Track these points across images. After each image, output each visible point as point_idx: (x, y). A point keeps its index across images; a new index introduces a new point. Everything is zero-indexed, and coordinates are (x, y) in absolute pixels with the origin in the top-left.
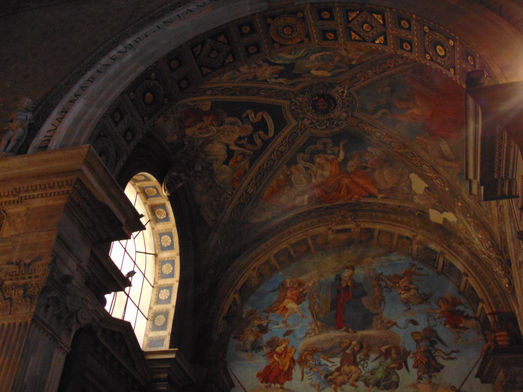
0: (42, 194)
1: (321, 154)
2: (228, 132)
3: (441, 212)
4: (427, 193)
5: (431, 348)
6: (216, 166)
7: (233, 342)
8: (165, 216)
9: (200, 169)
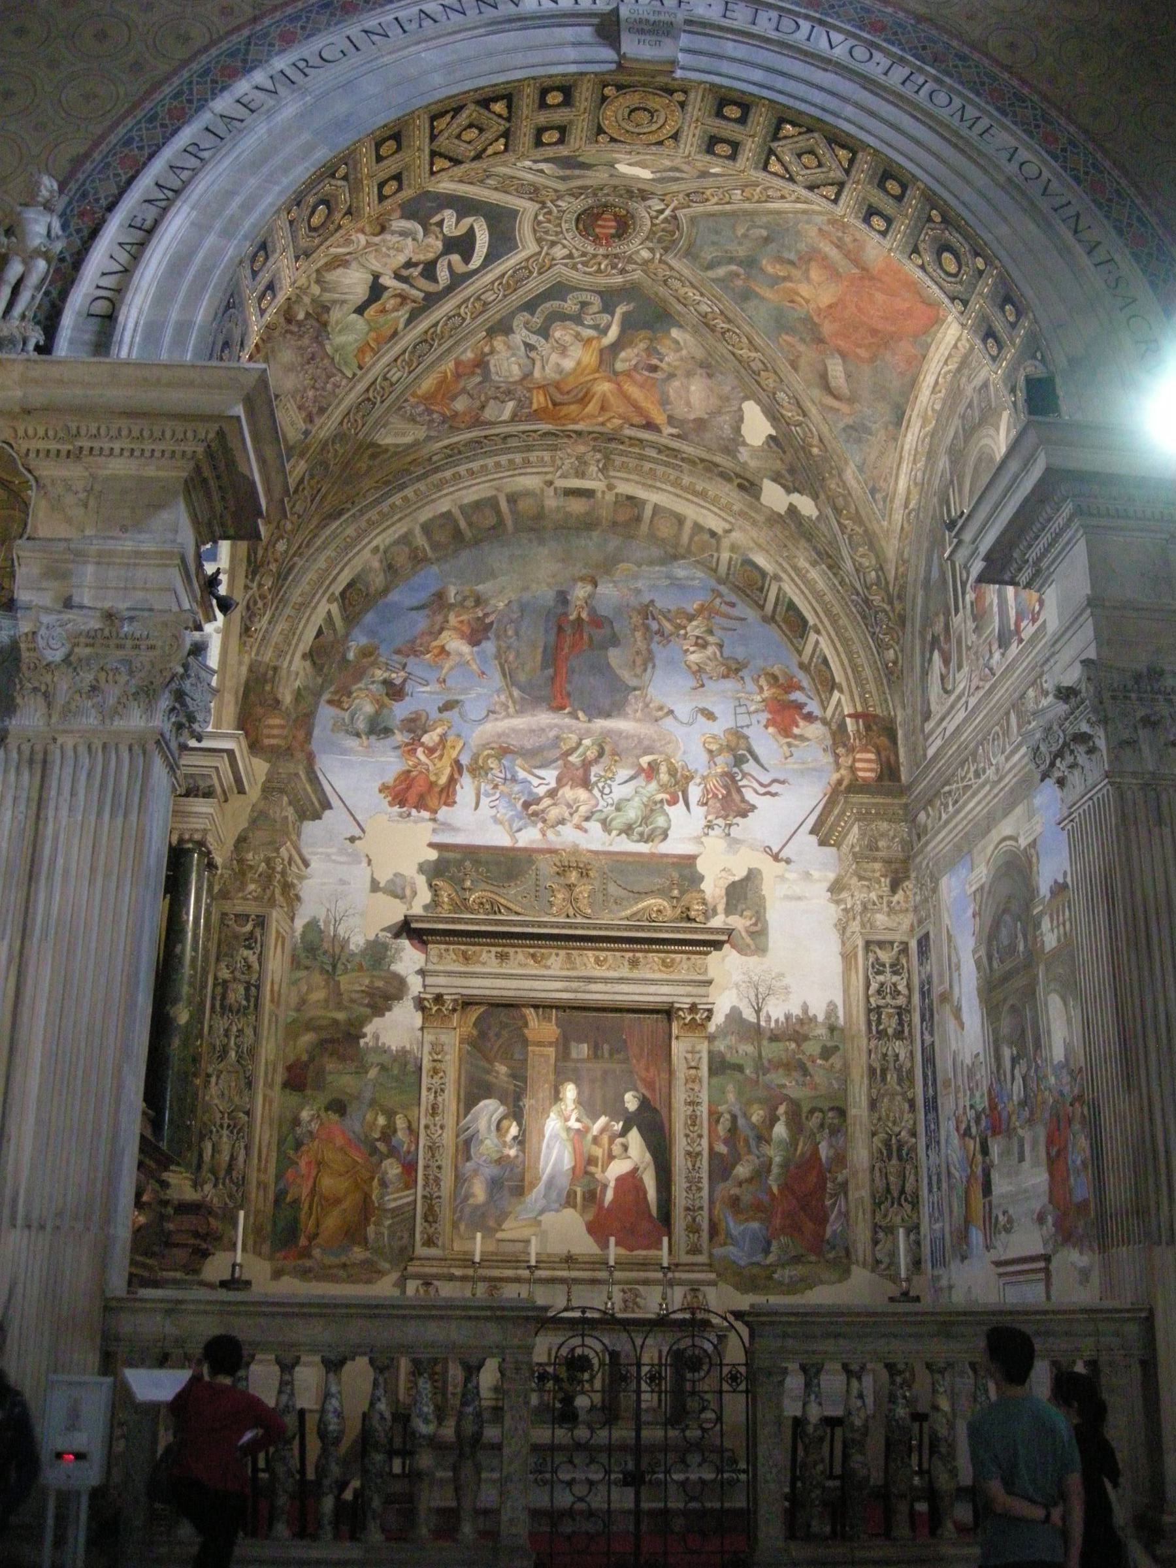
0: (132, 450)
3: (789, 491)
5: (735, 770)
6: (335, 315)
7: (326, 714)
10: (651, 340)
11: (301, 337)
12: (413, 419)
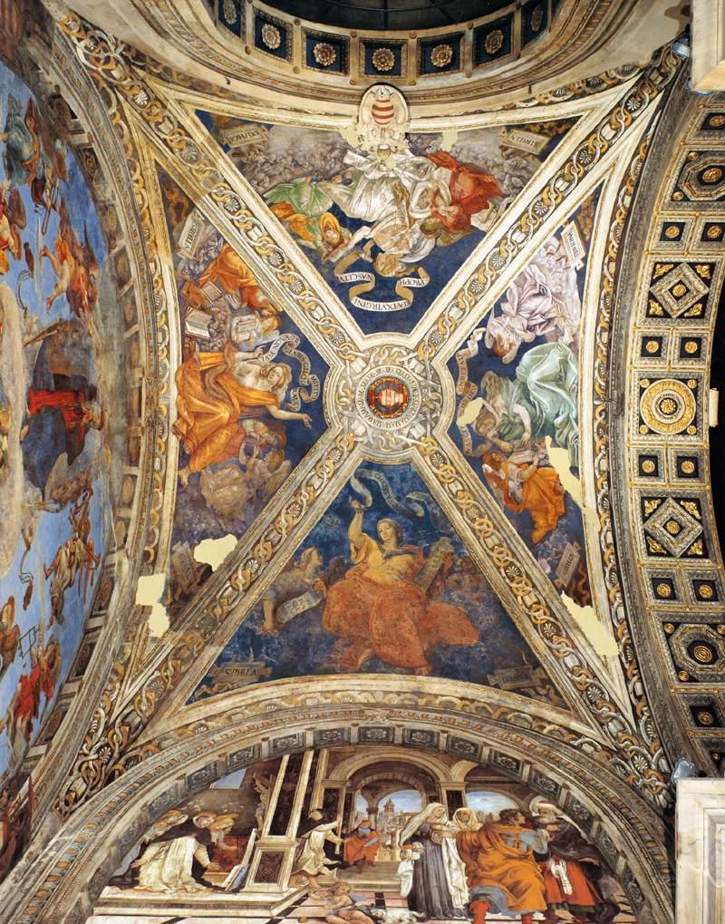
1: (291, 377)
2: (402, 235)
4: (198, 570)
6: (337, 190)
8: (317, 60)
9: (347, 161)
10: (278, 447)
11: (325, 158)
12: (205, 246)
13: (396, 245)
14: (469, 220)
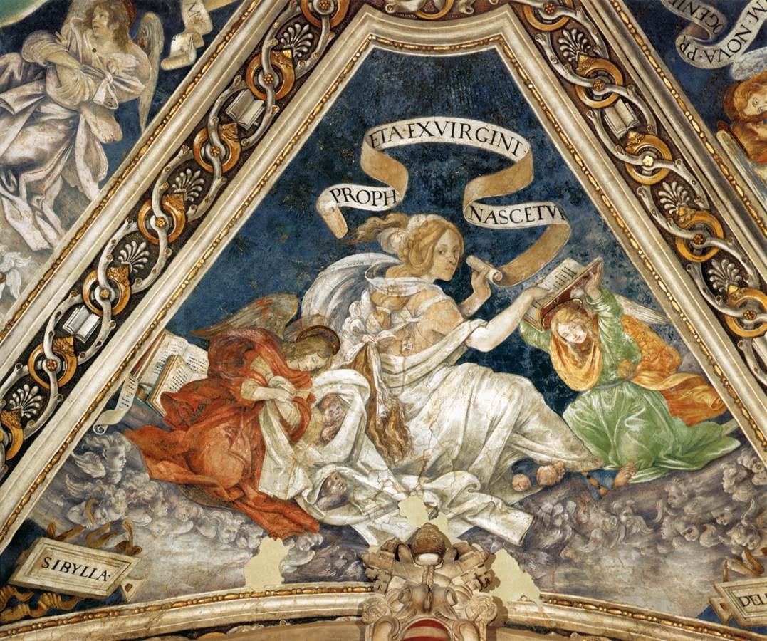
2: (390, 326)
9: (522, 520)
13: (404, 302)
14: (213, 361)
